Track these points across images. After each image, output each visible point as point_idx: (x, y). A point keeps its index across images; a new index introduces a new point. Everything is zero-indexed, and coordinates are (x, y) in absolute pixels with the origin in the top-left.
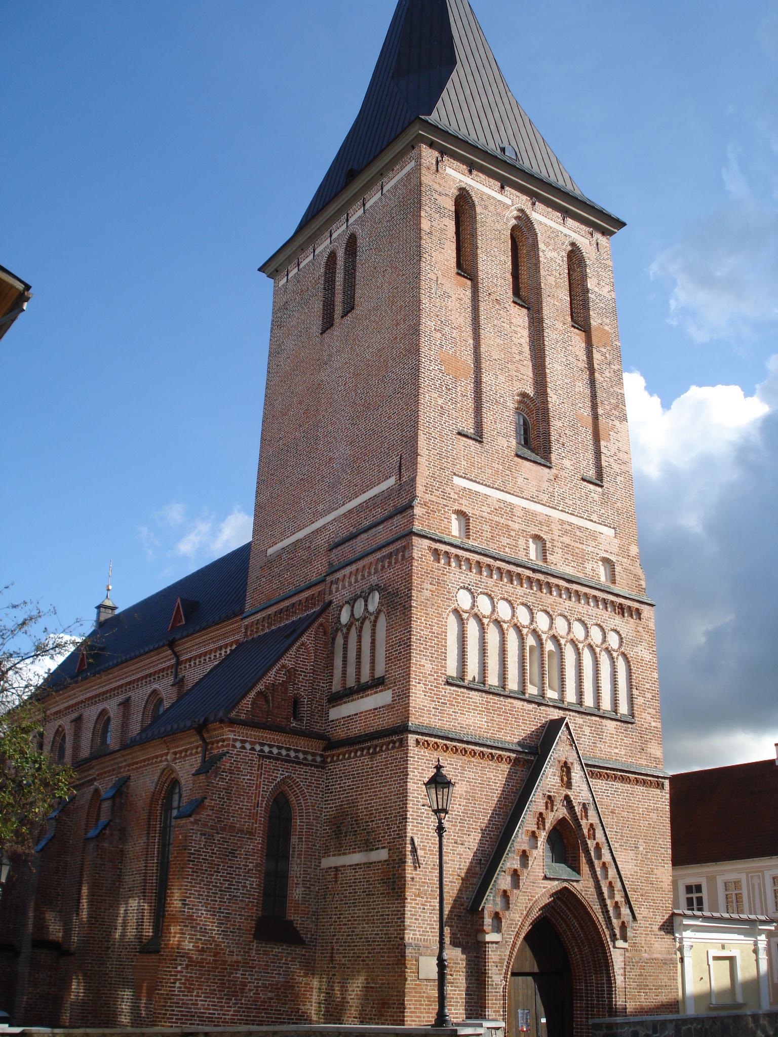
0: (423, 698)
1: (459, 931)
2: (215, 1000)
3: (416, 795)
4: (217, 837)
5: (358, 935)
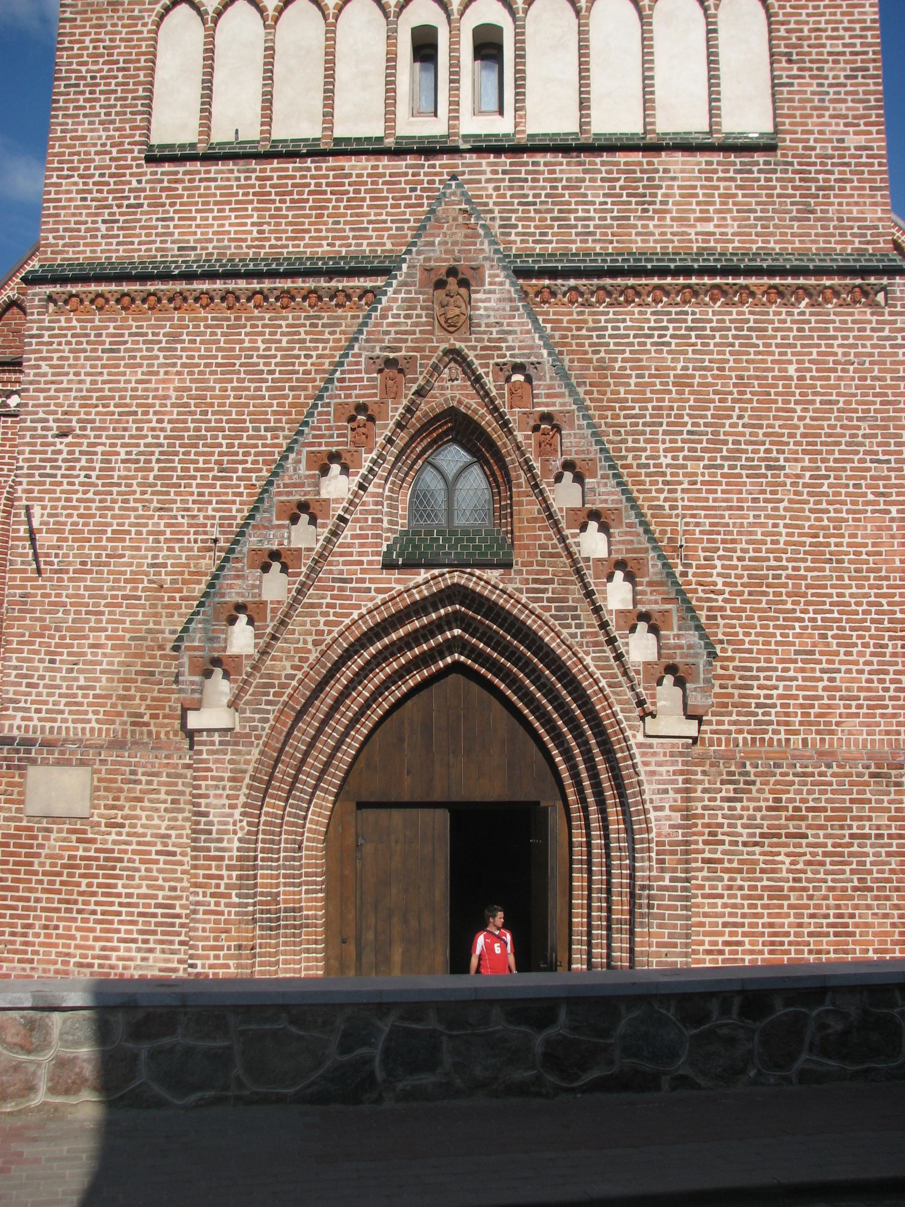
0: (76, 207)
1: (148, 707)
3: (41, 415)
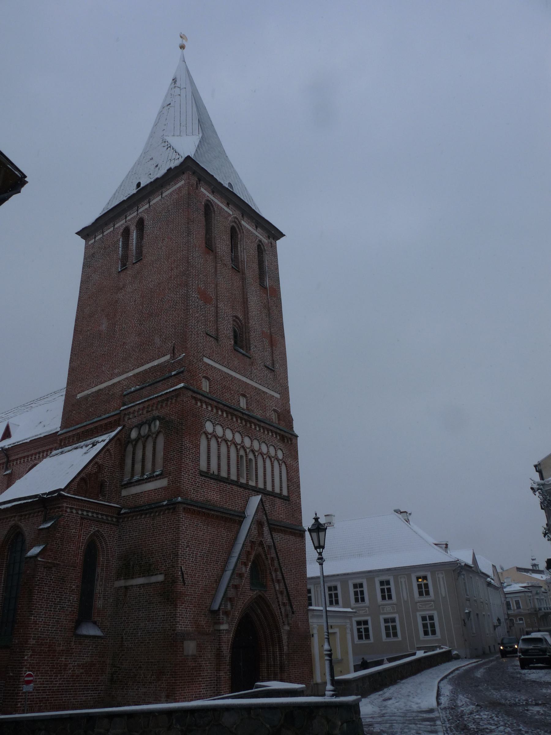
0: (187, 483)
2: (48, 677)
3: (183, 541)
4: (54, 569)
5: (142, 629)
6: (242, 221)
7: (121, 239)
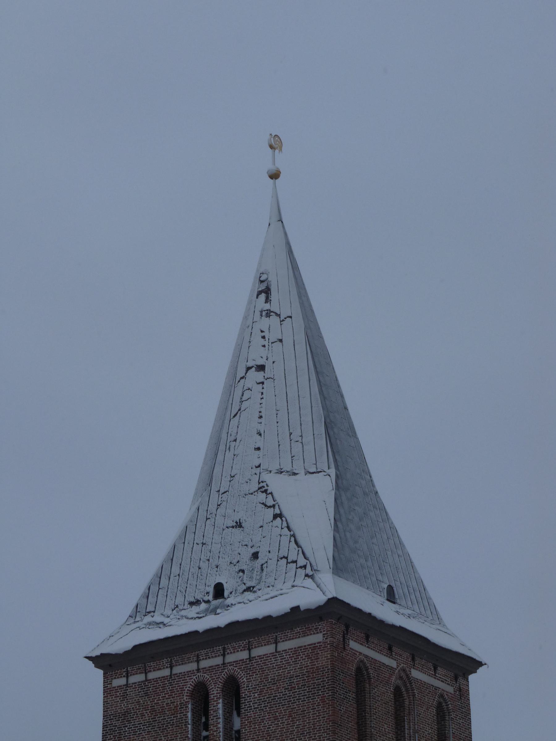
6: (412, 670)
7: (190, 706)
